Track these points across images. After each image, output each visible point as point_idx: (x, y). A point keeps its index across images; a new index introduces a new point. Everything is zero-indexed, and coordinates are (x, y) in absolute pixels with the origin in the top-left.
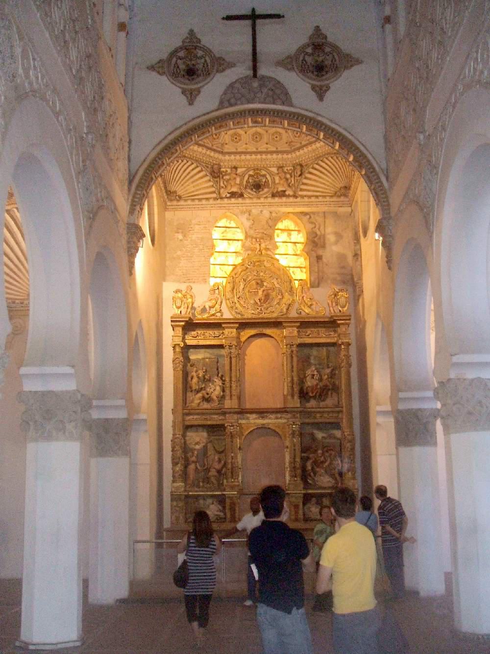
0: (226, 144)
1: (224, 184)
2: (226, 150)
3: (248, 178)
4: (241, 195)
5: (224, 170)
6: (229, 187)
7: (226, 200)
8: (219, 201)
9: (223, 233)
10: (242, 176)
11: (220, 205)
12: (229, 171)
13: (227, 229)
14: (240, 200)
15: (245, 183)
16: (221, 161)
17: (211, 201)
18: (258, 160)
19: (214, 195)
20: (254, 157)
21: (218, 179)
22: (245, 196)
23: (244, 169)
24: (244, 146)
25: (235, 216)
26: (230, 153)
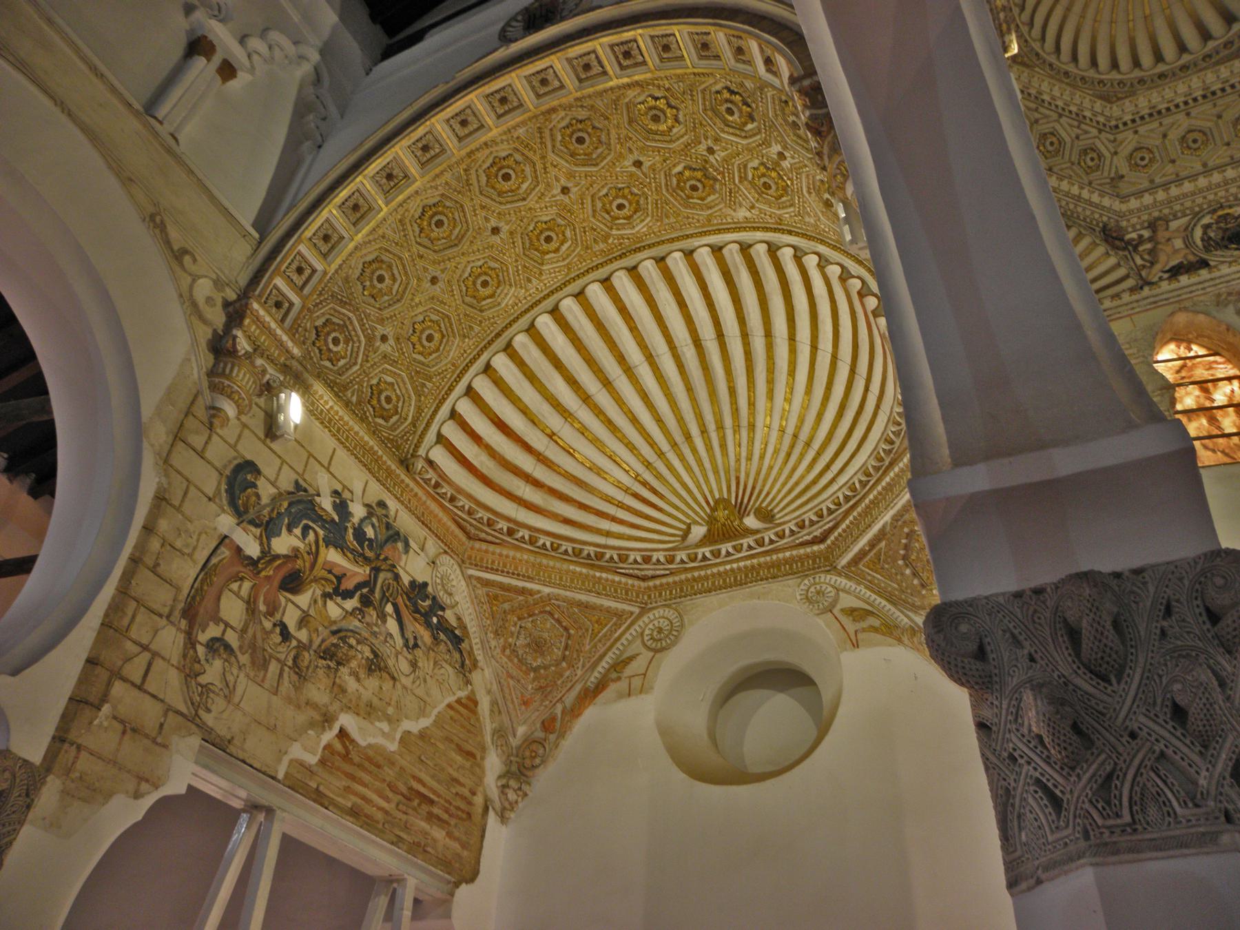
0: (1122, 177)
1: (1143, 259)
2: (1124, 192)
3: (1205, 233)
4: (1204, 264)
5: (1134, 235)
6: (1162, 258)
7: (1165, 286)
8: (1146, 291)
9: (1178, 372)
10: (1188, 230)
11: (1152, 300)
12: (1146, 234)
13: (1189, 363)
14: (1204, 273)
15: (1199, 243)
16: (1122, 215)
17: (1126, 297)
18: (1218, 185)
19: (1130, 283)
20: (1202, 182)
21: (1126, 253)
22: (1212, 263)
23: (1185, 220)
24: (1170, 168)
25: (1201, 317)
26: (1139, 194)
